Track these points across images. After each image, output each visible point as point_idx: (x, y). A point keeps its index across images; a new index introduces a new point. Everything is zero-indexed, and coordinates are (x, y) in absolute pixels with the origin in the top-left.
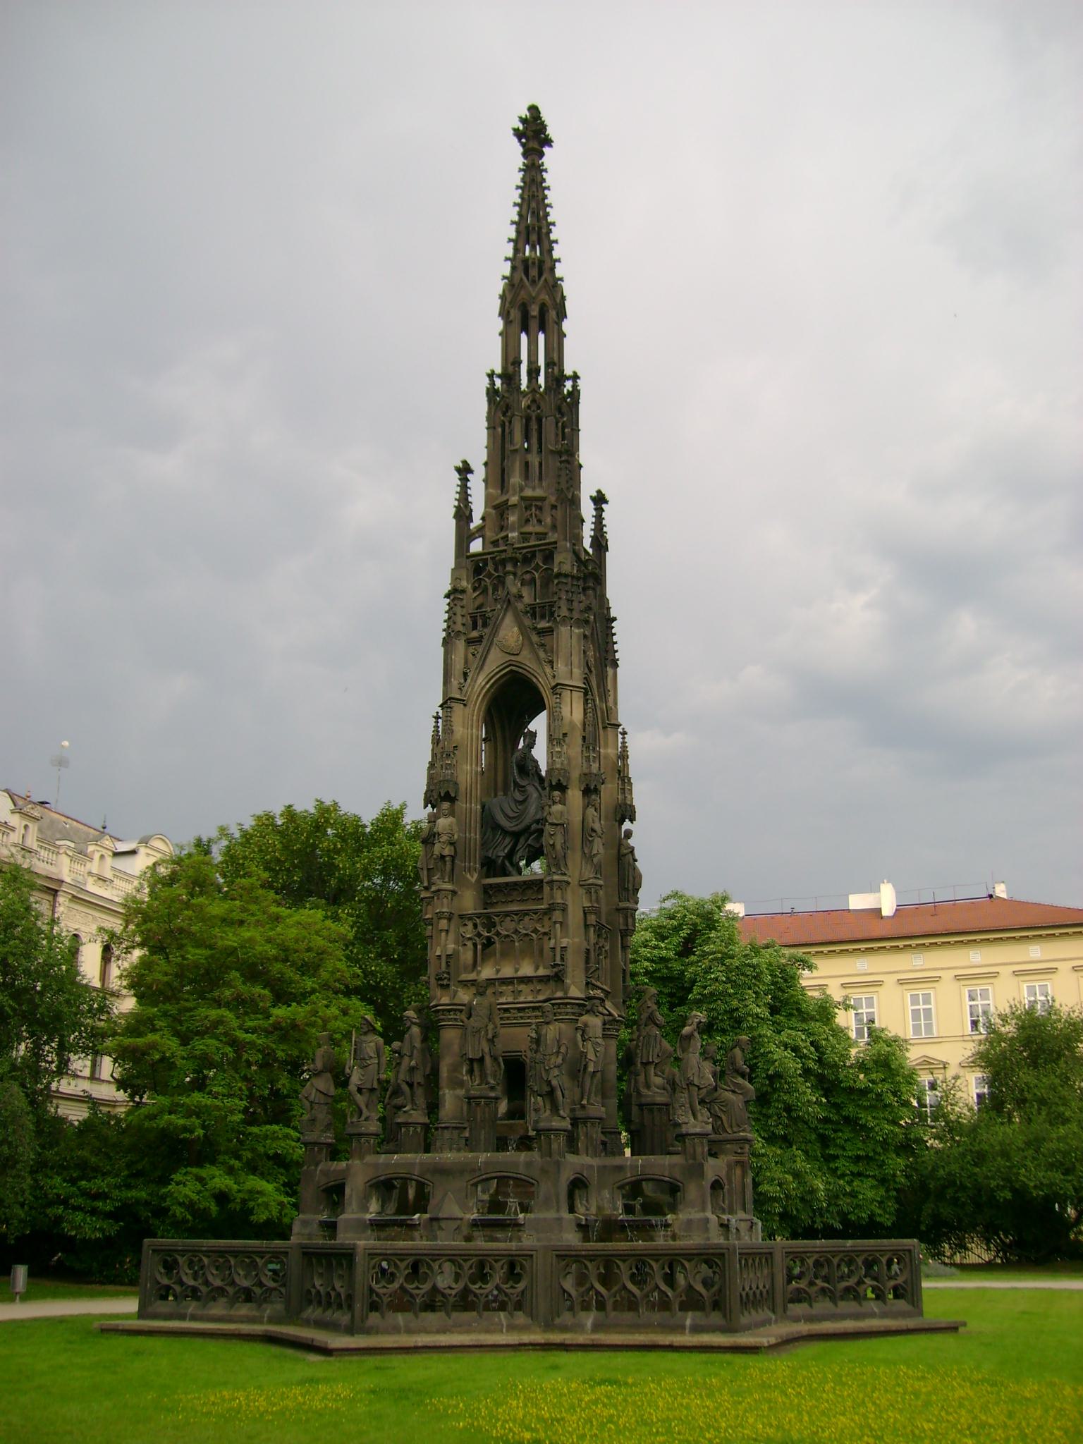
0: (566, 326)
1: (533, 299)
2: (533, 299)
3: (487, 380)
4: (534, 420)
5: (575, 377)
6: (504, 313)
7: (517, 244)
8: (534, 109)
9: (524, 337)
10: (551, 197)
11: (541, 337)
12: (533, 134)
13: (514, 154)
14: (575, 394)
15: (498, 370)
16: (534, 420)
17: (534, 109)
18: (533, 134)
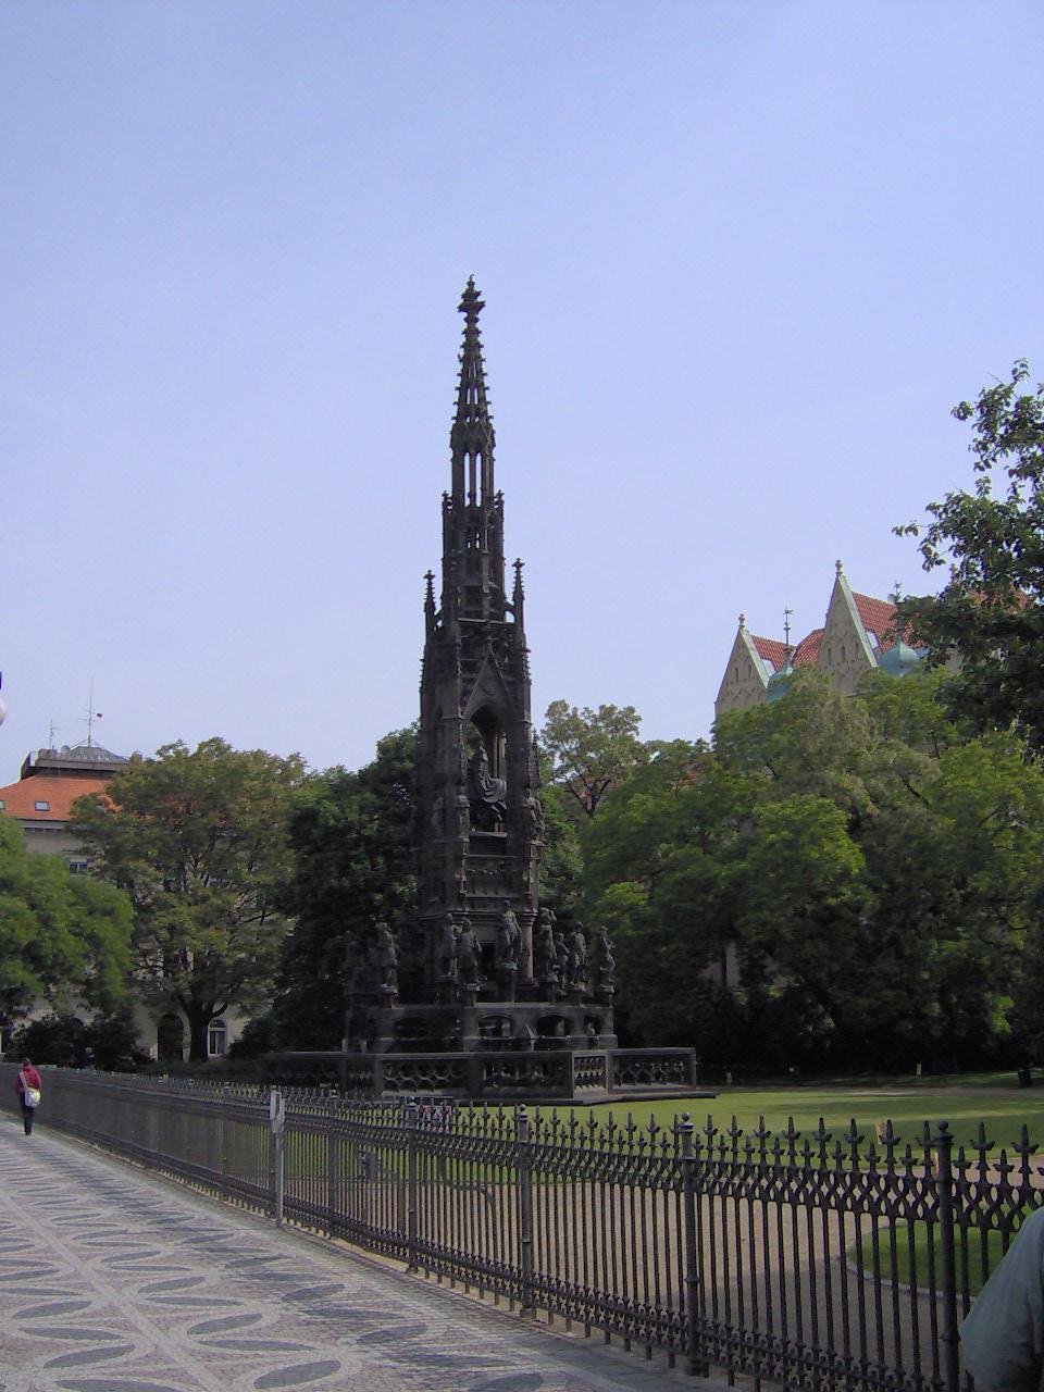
0: (496, 453)
1: (472, 434)
2: (472, 434)
3: (442, 499)
4: (472, 529)
5: (500, 495)
6: (453, 445)
7: (462, 390)
8: (471, 284)
9: (467, 458)
10: (483, 353)
11: (479, 457)
12: (471, 304)
13: (459, 322)
14: (501, 503)
15: (450, 495)
16: (472, 529)
17: (471, 284)
18: (471, 304)
